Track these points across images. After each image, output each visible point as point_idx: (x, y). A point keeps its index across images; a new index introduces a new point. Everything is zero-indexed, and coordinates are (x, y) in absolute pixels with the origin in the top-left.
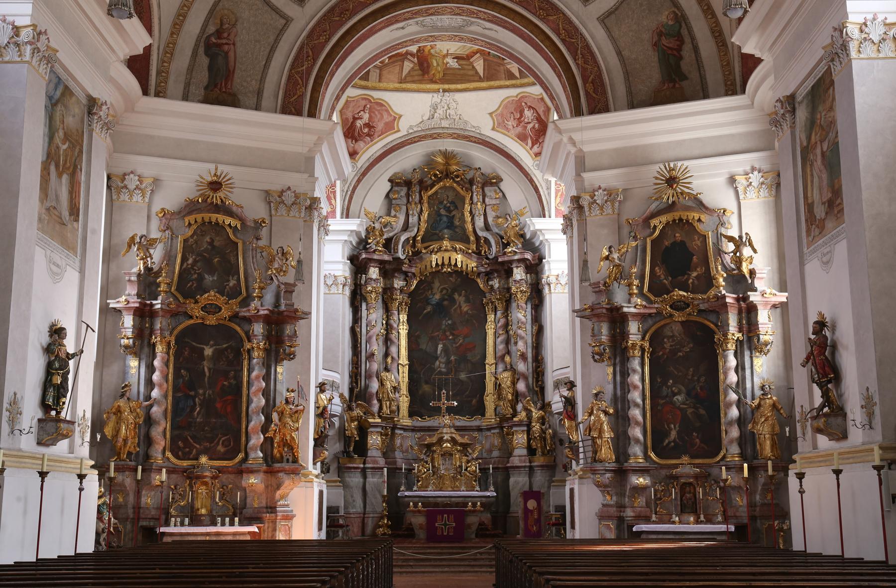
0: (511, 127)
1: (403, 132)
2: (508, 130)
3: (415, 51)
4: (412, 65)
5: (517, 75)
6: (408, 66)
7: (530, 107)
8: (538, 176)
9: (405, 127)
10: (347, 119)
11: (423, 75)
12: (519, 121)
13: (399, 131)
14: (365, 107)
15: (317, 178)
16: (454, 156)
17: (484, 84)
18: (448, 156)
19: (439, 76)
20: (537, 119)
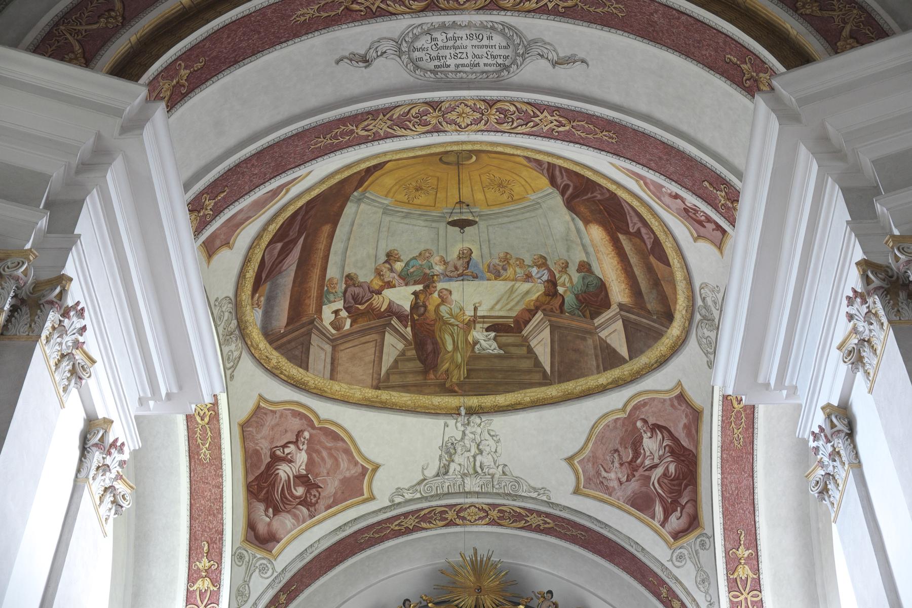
0: (615, 484)
1: (382, 501)
2: (609, 491)
3: (407, 307)
4: (400, 346)
5: (623, 351)
6: (393, 346)
7: (655, 428)
8: (684, 576)
9: (386, 491)
10: (257, 453)
11: (425, 372)
12: (632, 466)
13: (372, 498)
14: (299, 434)
15: (79, 236)
16: (494, 565)
17: (553, 391)
18: (479, 567)
19: (458, 376)
20: (672, 452)
